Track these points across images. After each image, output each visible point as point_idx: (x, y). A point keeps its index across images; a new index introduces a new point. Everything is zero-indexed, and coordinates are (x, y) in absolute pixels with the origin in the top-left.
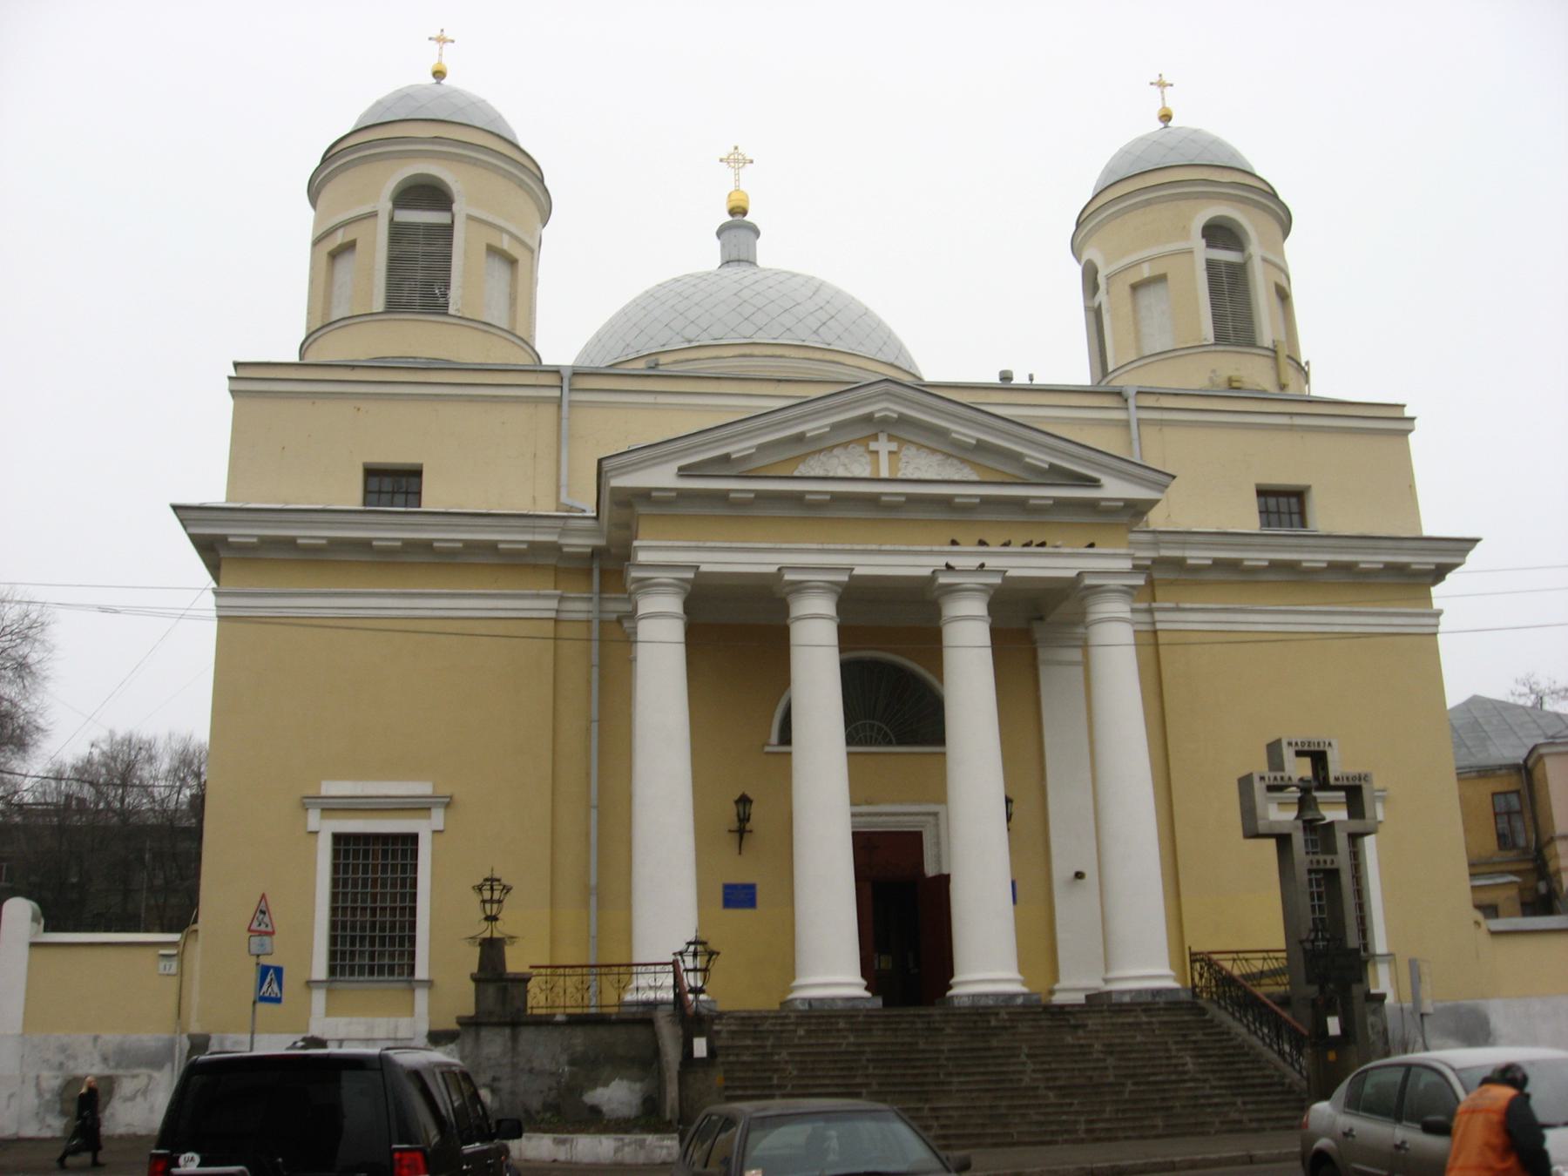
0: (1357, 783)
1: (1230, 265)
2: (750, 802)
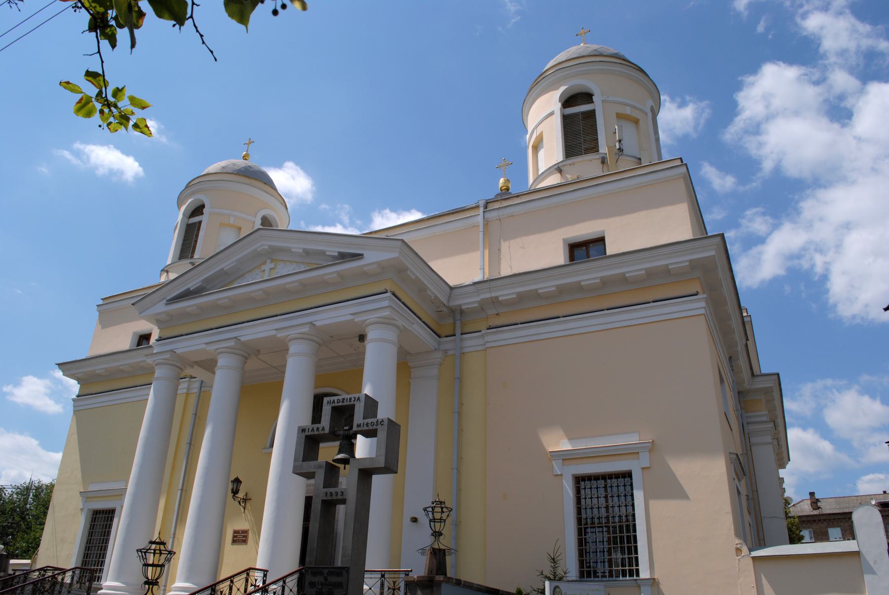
0: (374, 427)
1: (583, 113)
2: (241, 482)
